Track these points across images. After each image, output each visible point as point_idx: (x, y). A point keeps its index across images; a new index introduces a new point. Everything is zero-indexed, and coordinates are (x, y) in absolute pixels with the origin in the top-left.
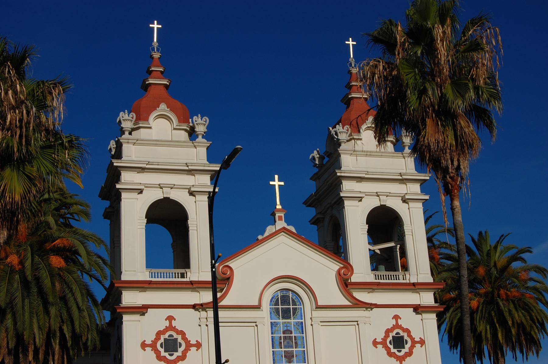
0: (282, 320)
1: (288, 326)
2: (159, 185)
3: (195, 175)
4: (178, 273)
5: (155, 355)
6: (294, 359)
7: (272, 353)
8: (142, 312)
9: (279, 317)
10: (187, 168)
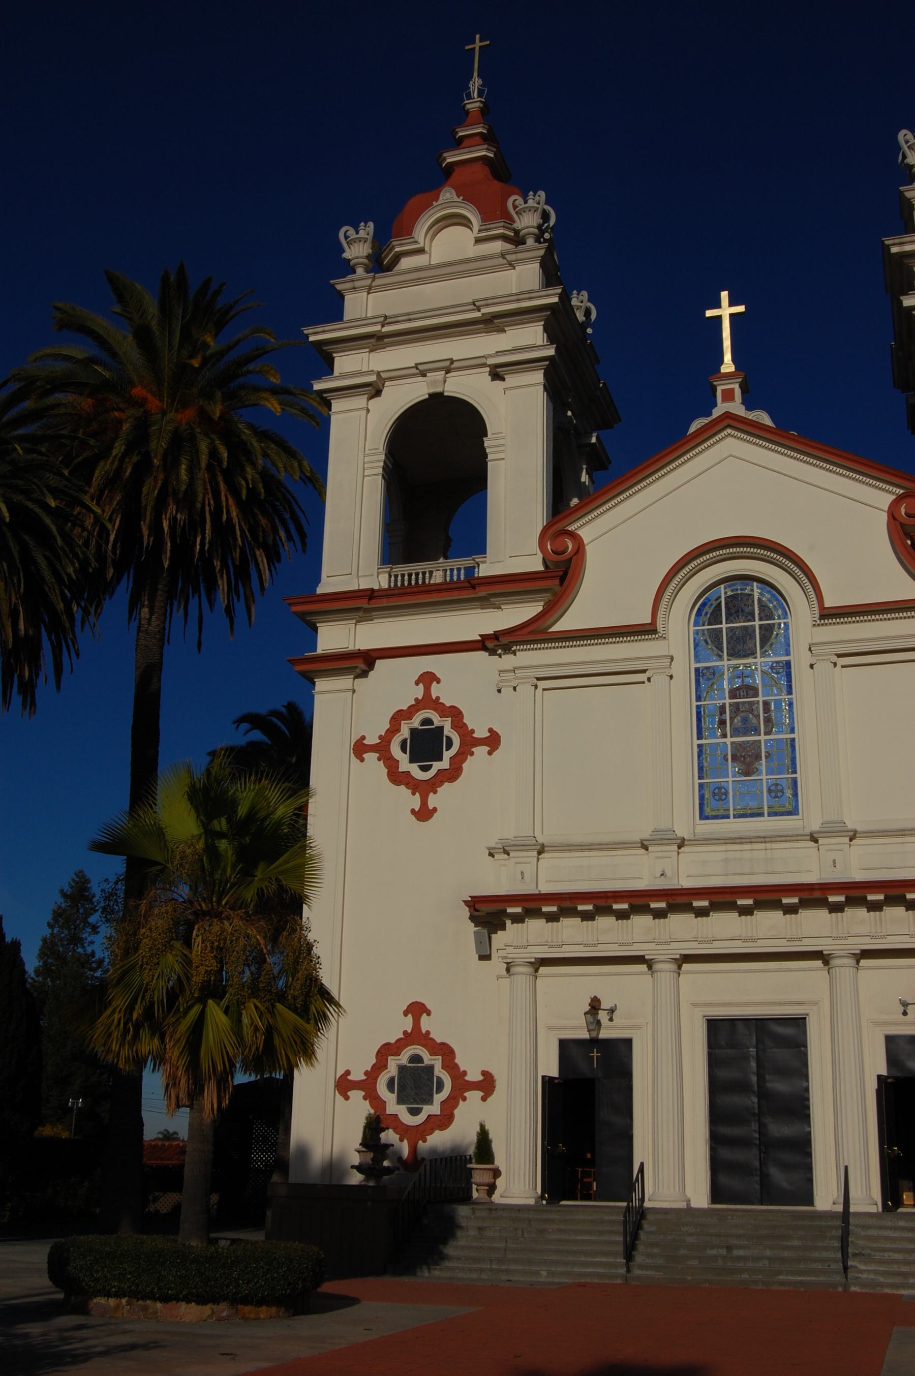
0: (729, 660)
1: (748, 677)
2: (416, 366)
3: (506, 329)
4: (459, 570)
5: (387, 770)
6: (761, 765)
7: (696, 750)
8: (356, 667)
9: (721, 654)
10: (477, 315)
